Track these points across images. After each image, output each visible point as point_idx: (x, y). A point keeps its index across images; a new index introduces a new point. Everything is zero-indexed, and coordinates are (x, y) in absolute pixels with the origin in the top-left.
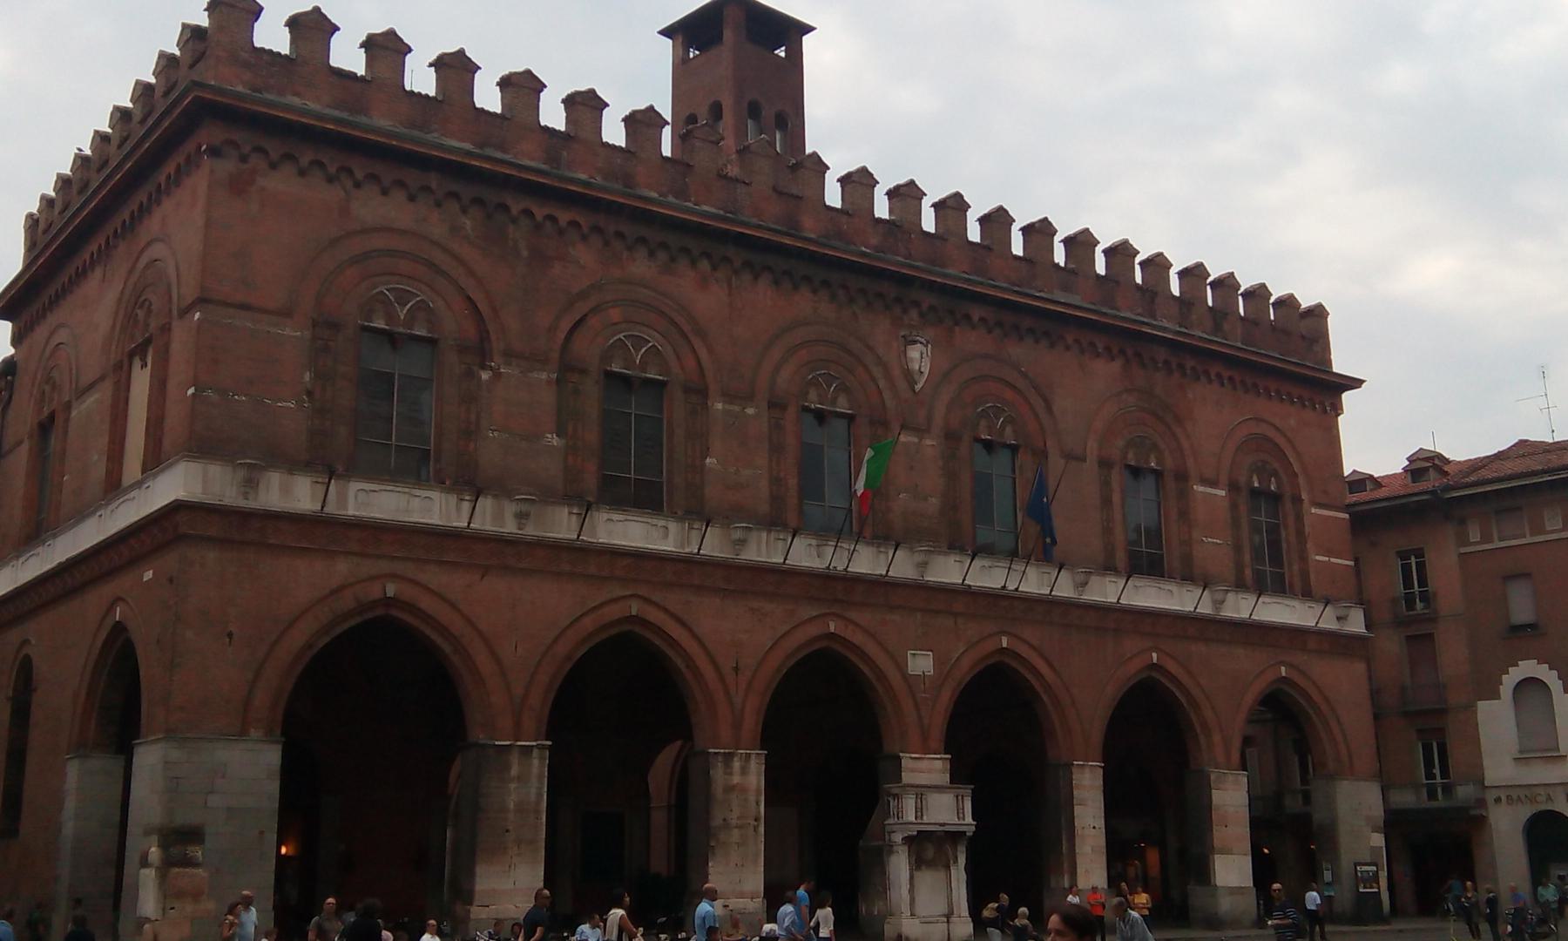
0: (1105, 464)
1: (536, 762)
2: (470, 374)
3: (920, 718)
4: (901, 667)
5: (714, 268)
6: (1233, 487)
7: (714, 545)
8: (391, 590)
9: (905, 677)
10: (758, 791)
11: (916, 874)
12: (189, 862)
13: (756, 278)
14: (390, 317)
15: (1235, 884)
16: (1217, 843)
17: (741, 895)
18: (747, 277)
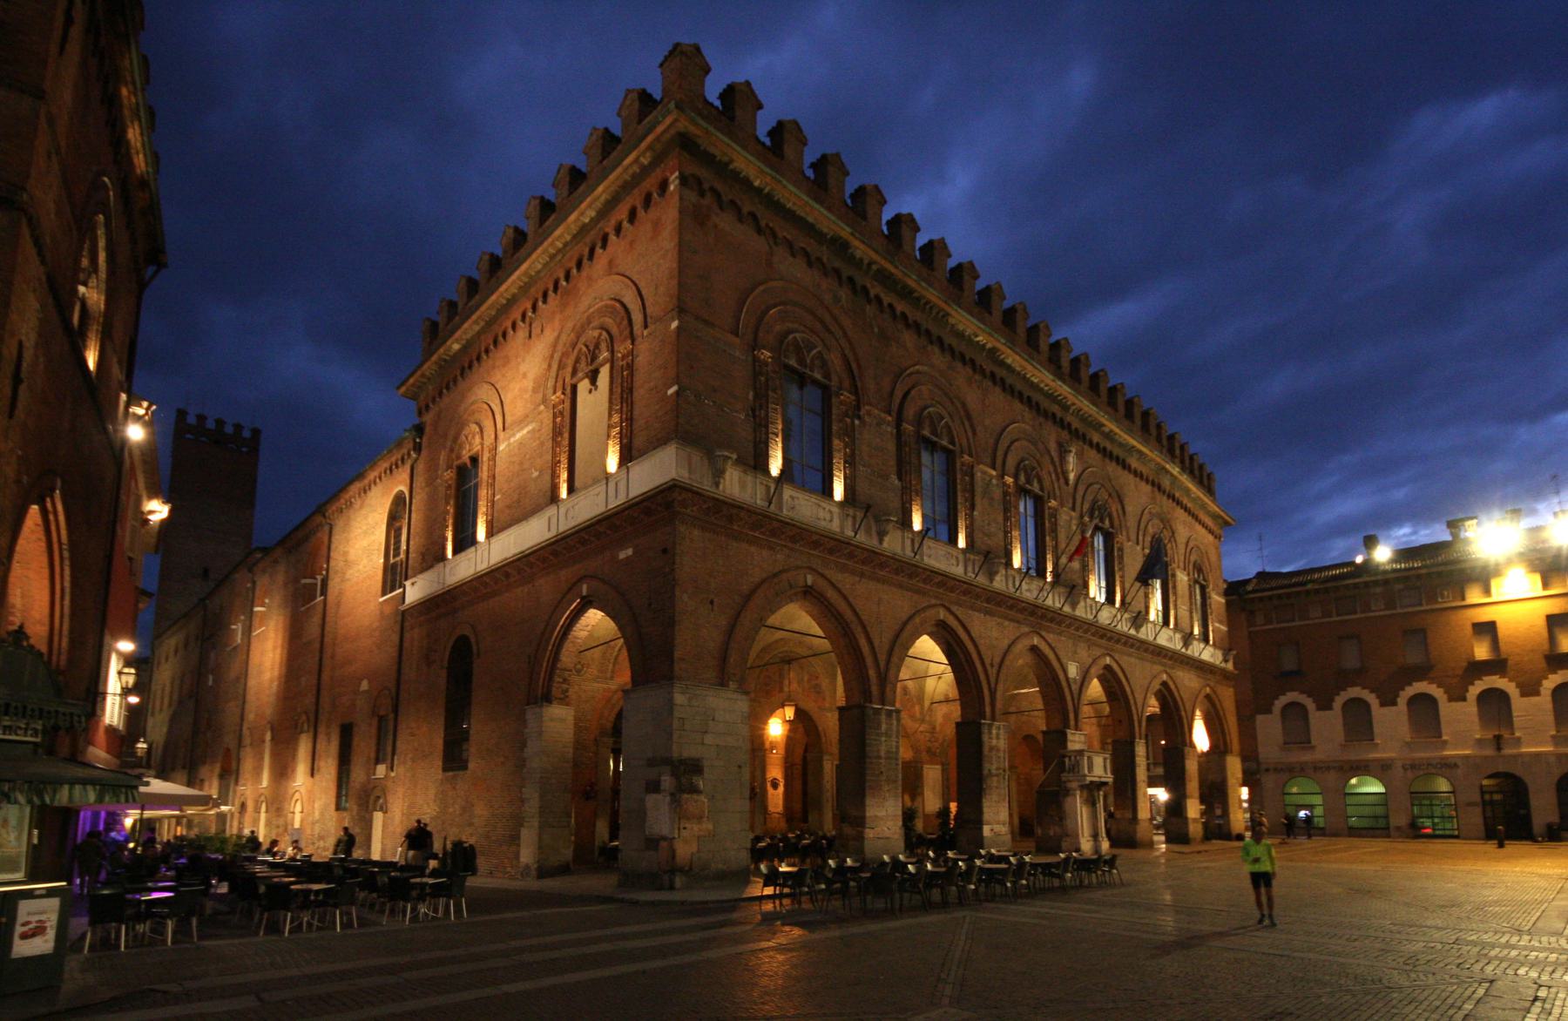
12: (694, 790)
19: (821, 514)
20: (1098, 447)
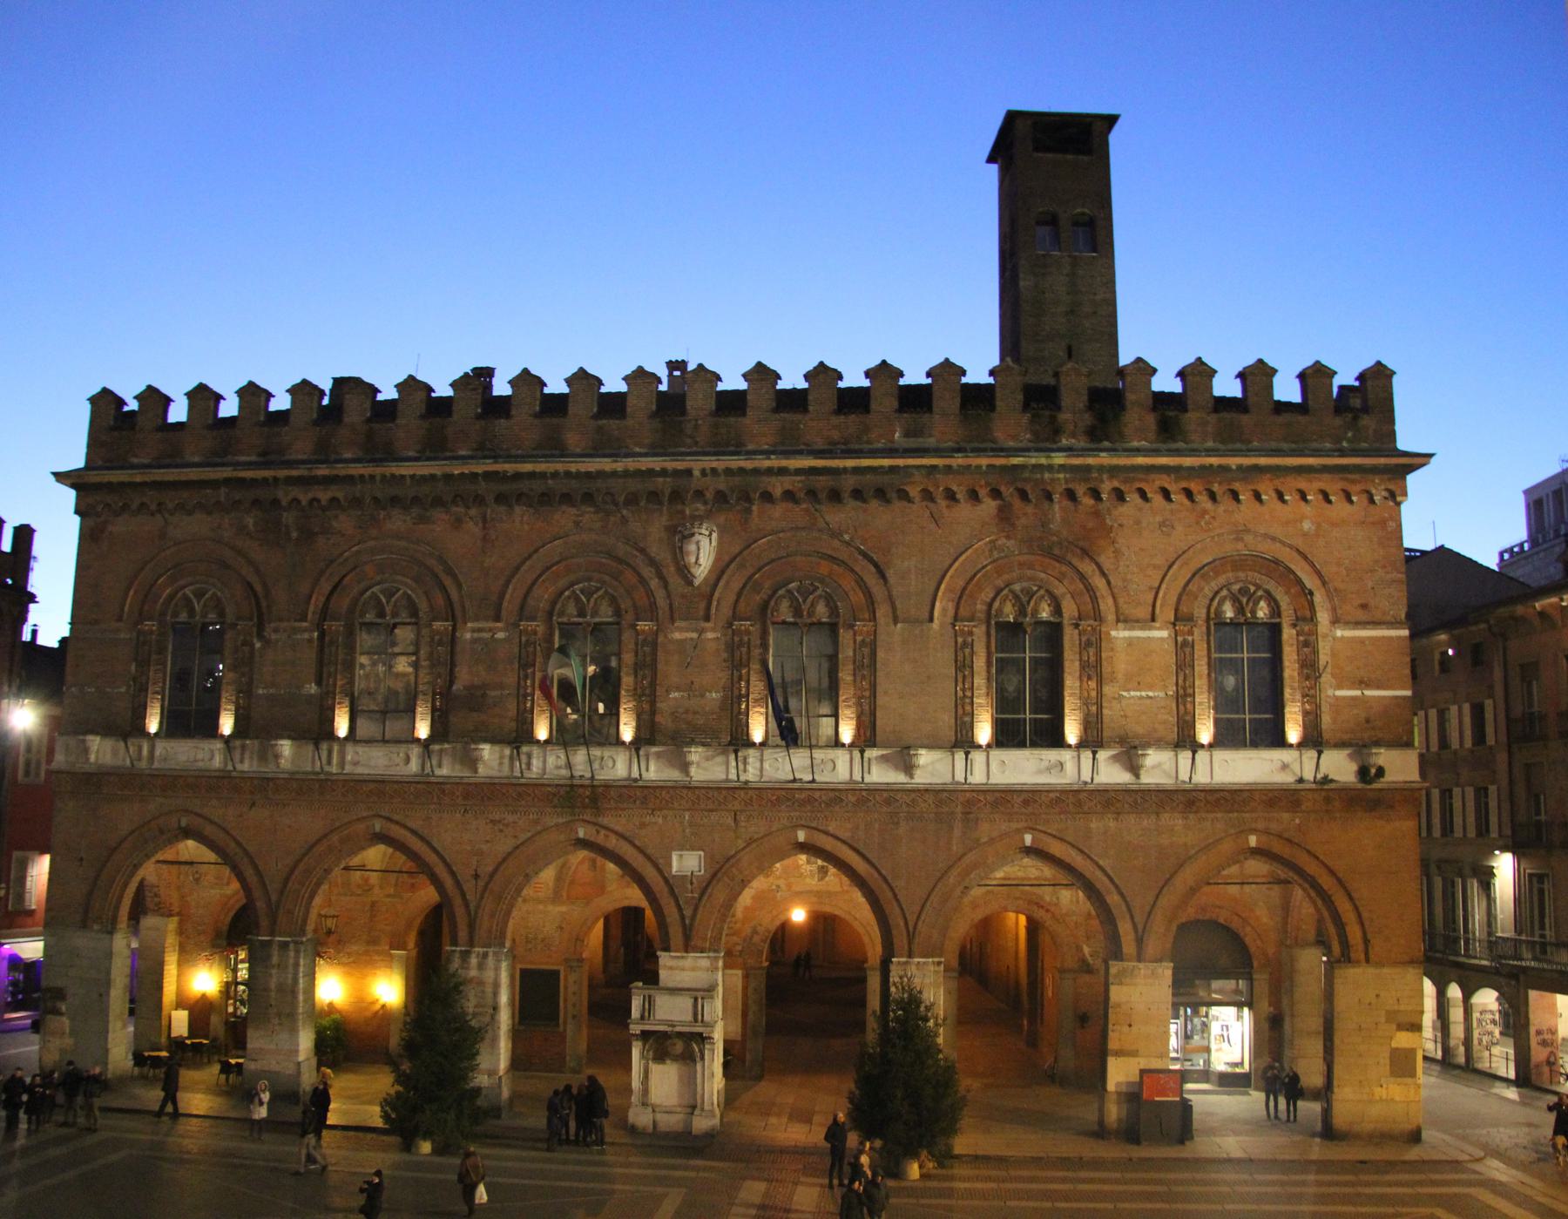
1: (292, 954)
3: (683, 918)
8: (183, 823)
11: (656, 1069)
14: (192, 612)
16: (1113, 1044)
18: (502, 509)
19: (200, 756)
20: (789, 496)
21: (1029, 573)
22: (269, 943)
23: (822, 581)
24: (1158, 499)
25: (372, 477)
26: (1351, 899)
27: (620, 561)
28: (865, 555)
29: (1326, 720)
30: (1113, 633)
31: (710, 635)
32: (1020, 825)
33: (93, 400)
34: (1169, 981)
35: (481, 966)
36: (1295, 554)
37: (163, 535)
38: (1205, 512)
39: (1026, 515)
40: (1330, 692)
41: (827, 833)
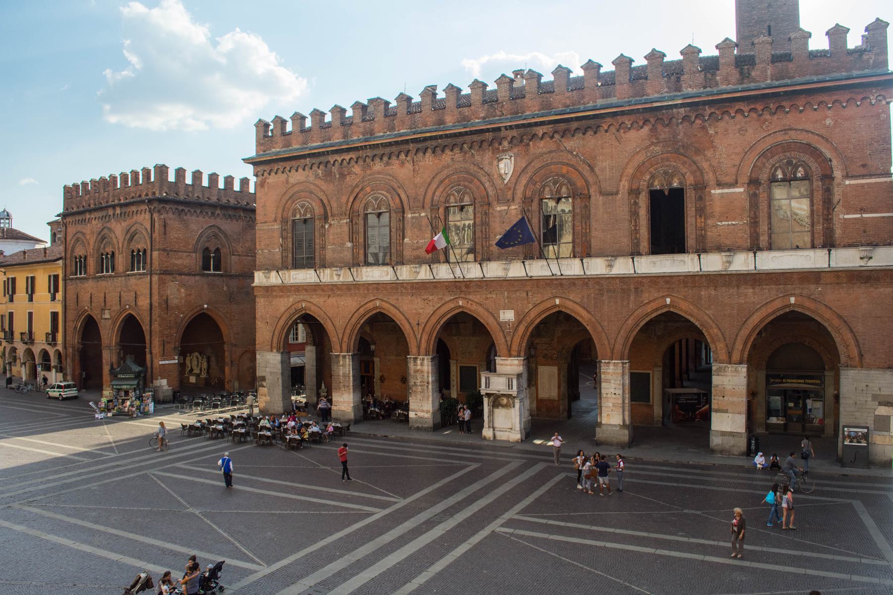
0: (634, 192)
2: (323, 227)
4: (496, 318)
5: (406, 156)
6: (754, 182)
7: (405, 273)
9: (499, 324)
10: (428, 373)
11: (496, 411)
13: (424, 153)
14: (300, 213)
15: (729, 430)
17: (423, 411)
21: (667, 163)
22: (338, 356)
23: (563, 176)
24: (739, 117)
25: (365, 146)
26: (852, 331)
27: (471, 174)
28: (584, 161)
29: (838, 232)
30: (713, 191)
31: (513, 207)
32: (666, 293)
33: (257, 125)
34: (745, 374)
35: (422, 365)
36: (820, 139)
37: (287, 182)
38: (766, 120)
39: (664, 133)
40: (841, 216)
41: (570, 300)
